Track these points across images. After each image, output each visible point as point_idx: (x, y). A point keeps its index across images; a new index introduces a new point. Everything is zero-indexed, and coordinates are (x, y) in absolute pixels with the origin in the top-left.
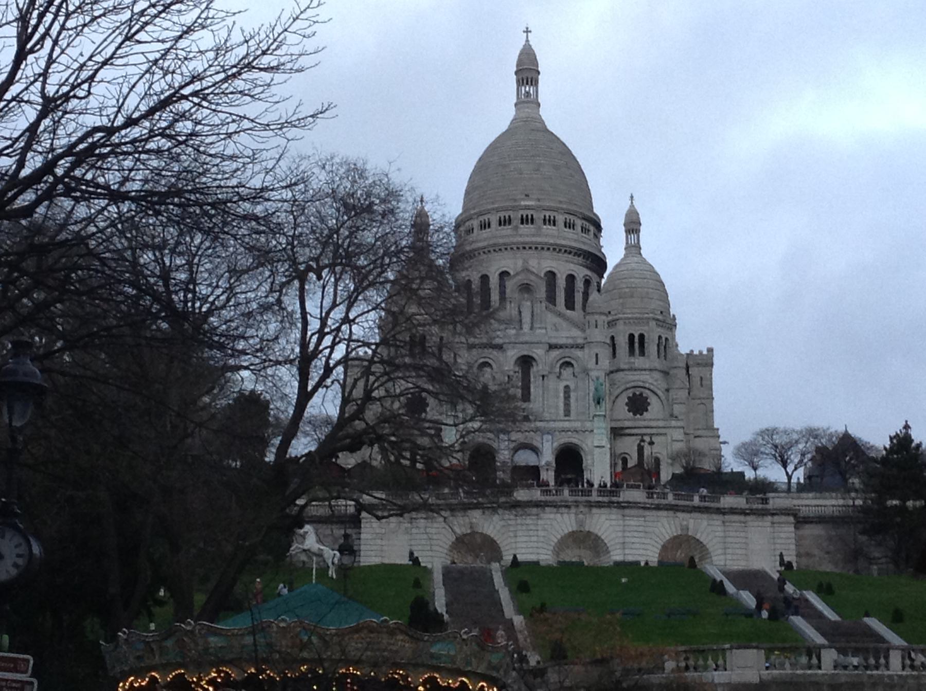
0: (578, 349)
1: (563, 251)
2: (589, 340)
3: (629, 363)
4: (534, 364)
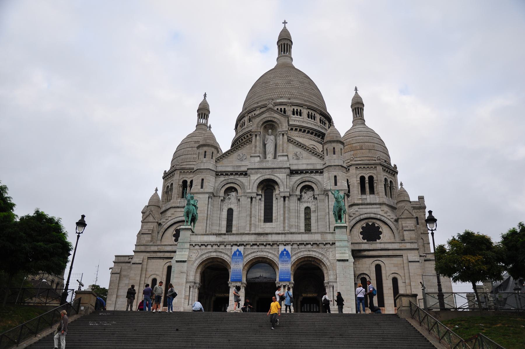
0: (318, 174)
1: (307, 131)
2: (327, 165)
4: (276, 187)
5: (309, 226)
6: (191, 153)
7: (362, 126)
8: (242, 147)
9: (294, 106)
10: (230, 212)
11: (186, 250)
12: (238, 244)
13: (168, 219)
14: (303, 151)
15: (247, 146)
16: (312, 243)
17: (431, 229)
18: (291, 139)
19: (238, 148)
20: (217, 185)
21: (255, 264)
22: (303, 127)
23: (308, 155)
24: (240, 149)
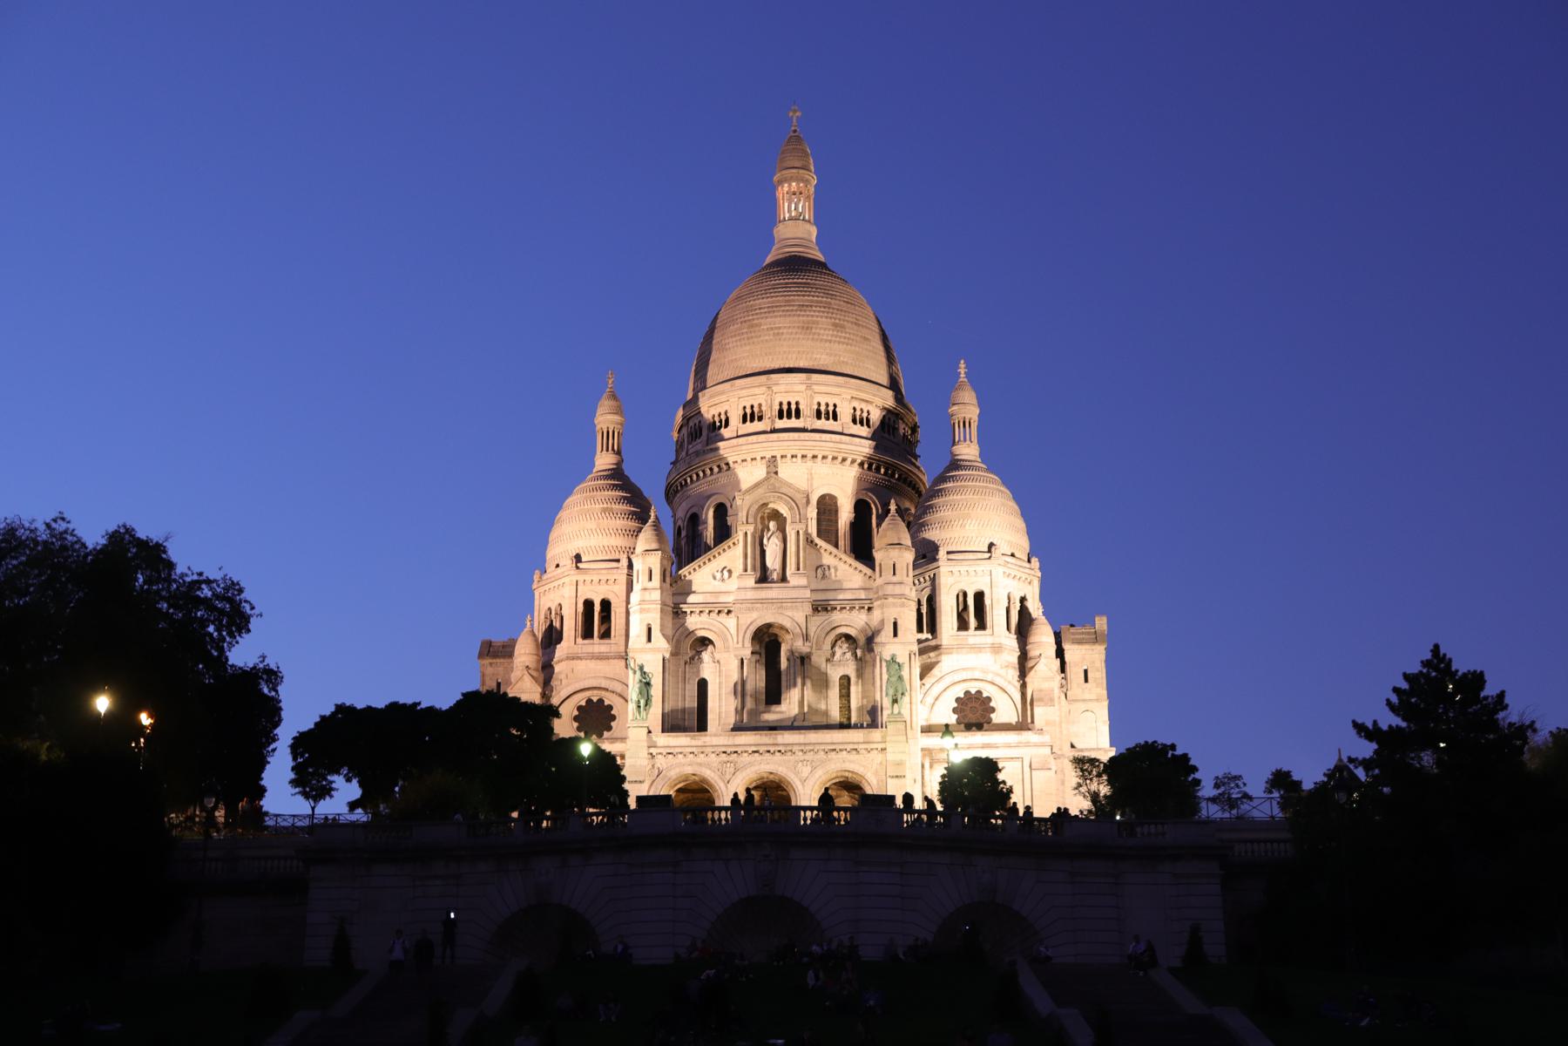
1: (849, 460)
4: (788, 637)
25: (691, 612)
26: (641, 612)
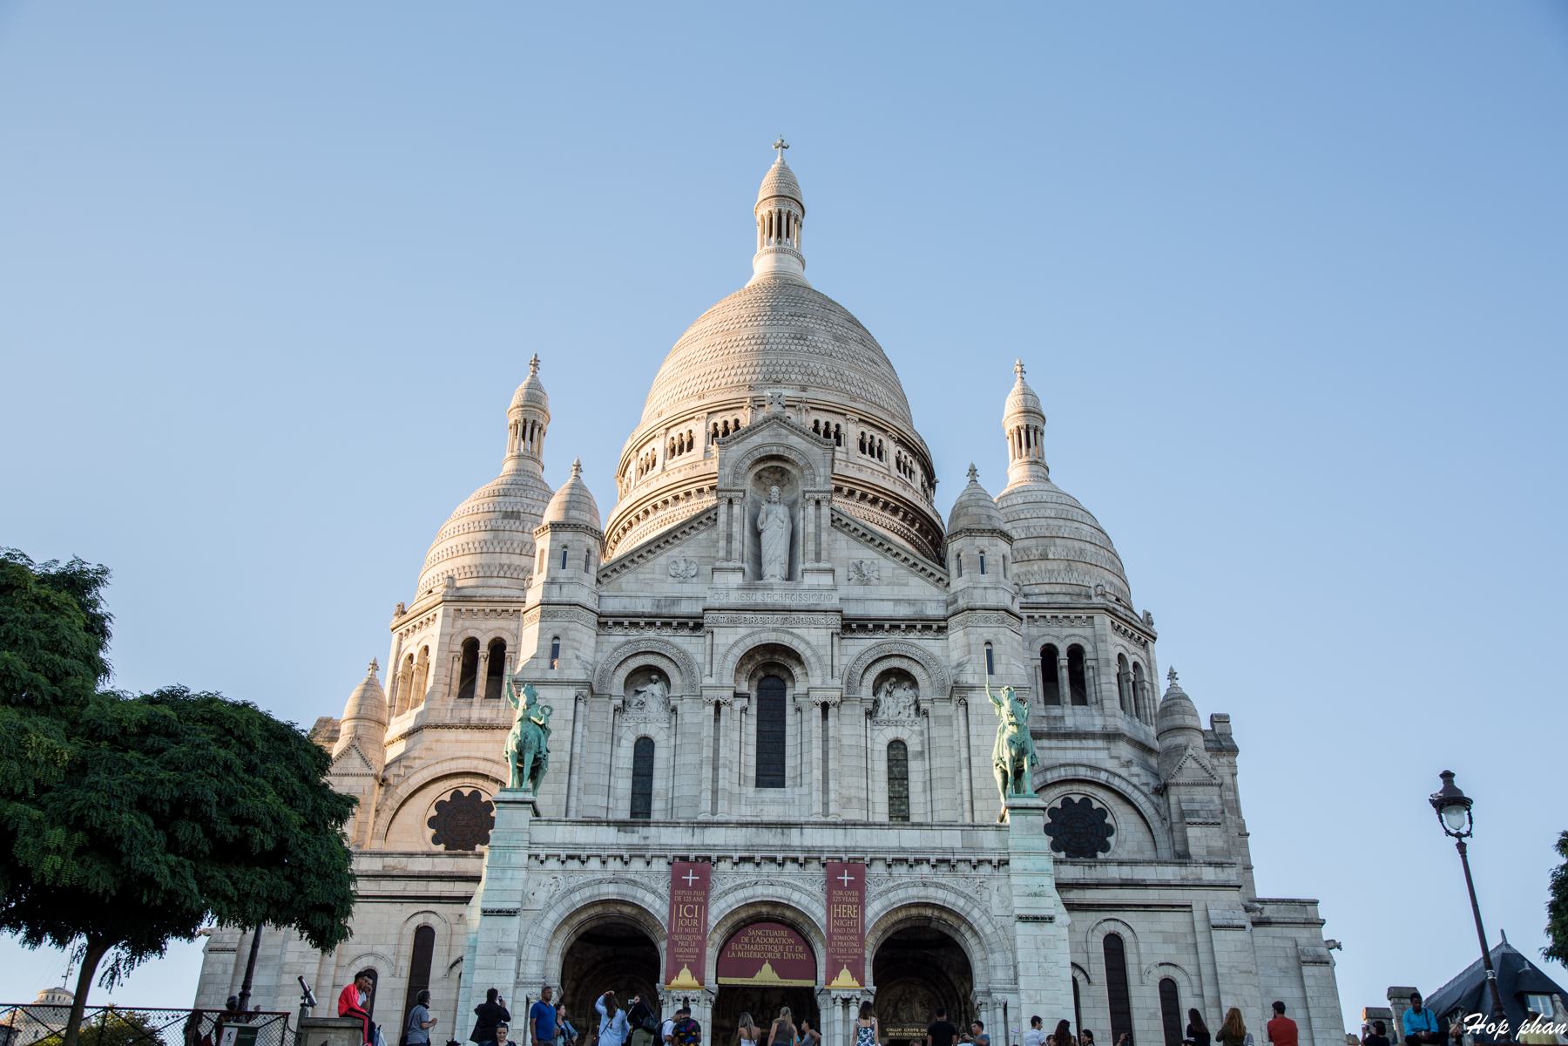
0: (929, 634)
1: (858, 493)
2: (962, 603)
3: (1047, 717)
4: (797, 671)
5: (903, 804)
6: (491, 550)
7: (1046, 486)
8: (685, 537)
9: (817, 412)
10: (644, 748)
11: (516, 872)
12: (692, 855)
13: (412, 767)
14: (879, 556)
15: (700, 537)
16: (933, 861)
17: (1454, 832)
18: (841, 517)
19: (671, 540)
20: (601, 657)
21: (745, 926)
22: (846, 481)
23: (896, 571)
24: (677, 542)
25: (631, 624)
26: (542, 616)
